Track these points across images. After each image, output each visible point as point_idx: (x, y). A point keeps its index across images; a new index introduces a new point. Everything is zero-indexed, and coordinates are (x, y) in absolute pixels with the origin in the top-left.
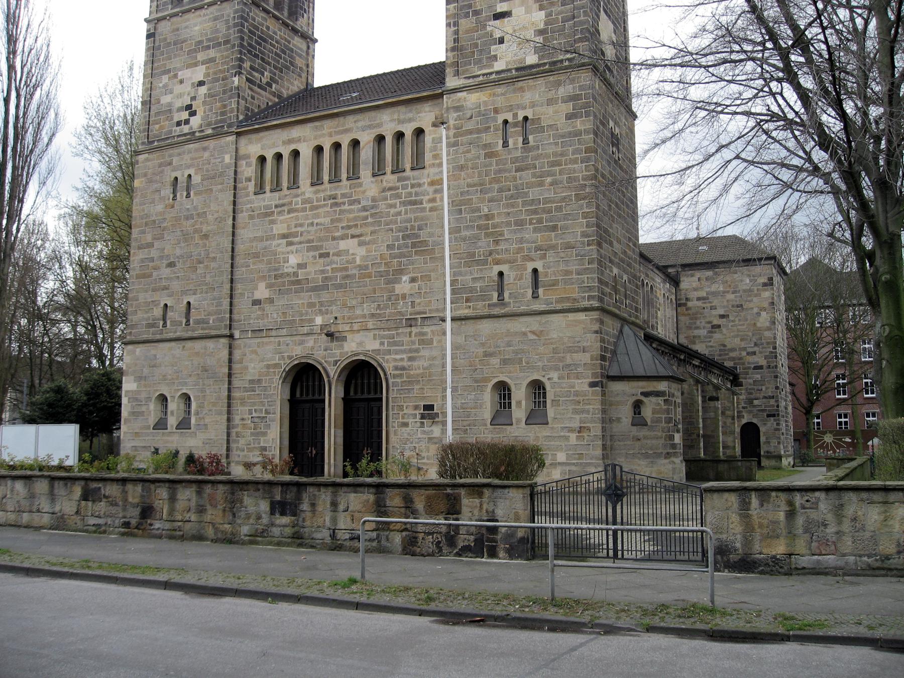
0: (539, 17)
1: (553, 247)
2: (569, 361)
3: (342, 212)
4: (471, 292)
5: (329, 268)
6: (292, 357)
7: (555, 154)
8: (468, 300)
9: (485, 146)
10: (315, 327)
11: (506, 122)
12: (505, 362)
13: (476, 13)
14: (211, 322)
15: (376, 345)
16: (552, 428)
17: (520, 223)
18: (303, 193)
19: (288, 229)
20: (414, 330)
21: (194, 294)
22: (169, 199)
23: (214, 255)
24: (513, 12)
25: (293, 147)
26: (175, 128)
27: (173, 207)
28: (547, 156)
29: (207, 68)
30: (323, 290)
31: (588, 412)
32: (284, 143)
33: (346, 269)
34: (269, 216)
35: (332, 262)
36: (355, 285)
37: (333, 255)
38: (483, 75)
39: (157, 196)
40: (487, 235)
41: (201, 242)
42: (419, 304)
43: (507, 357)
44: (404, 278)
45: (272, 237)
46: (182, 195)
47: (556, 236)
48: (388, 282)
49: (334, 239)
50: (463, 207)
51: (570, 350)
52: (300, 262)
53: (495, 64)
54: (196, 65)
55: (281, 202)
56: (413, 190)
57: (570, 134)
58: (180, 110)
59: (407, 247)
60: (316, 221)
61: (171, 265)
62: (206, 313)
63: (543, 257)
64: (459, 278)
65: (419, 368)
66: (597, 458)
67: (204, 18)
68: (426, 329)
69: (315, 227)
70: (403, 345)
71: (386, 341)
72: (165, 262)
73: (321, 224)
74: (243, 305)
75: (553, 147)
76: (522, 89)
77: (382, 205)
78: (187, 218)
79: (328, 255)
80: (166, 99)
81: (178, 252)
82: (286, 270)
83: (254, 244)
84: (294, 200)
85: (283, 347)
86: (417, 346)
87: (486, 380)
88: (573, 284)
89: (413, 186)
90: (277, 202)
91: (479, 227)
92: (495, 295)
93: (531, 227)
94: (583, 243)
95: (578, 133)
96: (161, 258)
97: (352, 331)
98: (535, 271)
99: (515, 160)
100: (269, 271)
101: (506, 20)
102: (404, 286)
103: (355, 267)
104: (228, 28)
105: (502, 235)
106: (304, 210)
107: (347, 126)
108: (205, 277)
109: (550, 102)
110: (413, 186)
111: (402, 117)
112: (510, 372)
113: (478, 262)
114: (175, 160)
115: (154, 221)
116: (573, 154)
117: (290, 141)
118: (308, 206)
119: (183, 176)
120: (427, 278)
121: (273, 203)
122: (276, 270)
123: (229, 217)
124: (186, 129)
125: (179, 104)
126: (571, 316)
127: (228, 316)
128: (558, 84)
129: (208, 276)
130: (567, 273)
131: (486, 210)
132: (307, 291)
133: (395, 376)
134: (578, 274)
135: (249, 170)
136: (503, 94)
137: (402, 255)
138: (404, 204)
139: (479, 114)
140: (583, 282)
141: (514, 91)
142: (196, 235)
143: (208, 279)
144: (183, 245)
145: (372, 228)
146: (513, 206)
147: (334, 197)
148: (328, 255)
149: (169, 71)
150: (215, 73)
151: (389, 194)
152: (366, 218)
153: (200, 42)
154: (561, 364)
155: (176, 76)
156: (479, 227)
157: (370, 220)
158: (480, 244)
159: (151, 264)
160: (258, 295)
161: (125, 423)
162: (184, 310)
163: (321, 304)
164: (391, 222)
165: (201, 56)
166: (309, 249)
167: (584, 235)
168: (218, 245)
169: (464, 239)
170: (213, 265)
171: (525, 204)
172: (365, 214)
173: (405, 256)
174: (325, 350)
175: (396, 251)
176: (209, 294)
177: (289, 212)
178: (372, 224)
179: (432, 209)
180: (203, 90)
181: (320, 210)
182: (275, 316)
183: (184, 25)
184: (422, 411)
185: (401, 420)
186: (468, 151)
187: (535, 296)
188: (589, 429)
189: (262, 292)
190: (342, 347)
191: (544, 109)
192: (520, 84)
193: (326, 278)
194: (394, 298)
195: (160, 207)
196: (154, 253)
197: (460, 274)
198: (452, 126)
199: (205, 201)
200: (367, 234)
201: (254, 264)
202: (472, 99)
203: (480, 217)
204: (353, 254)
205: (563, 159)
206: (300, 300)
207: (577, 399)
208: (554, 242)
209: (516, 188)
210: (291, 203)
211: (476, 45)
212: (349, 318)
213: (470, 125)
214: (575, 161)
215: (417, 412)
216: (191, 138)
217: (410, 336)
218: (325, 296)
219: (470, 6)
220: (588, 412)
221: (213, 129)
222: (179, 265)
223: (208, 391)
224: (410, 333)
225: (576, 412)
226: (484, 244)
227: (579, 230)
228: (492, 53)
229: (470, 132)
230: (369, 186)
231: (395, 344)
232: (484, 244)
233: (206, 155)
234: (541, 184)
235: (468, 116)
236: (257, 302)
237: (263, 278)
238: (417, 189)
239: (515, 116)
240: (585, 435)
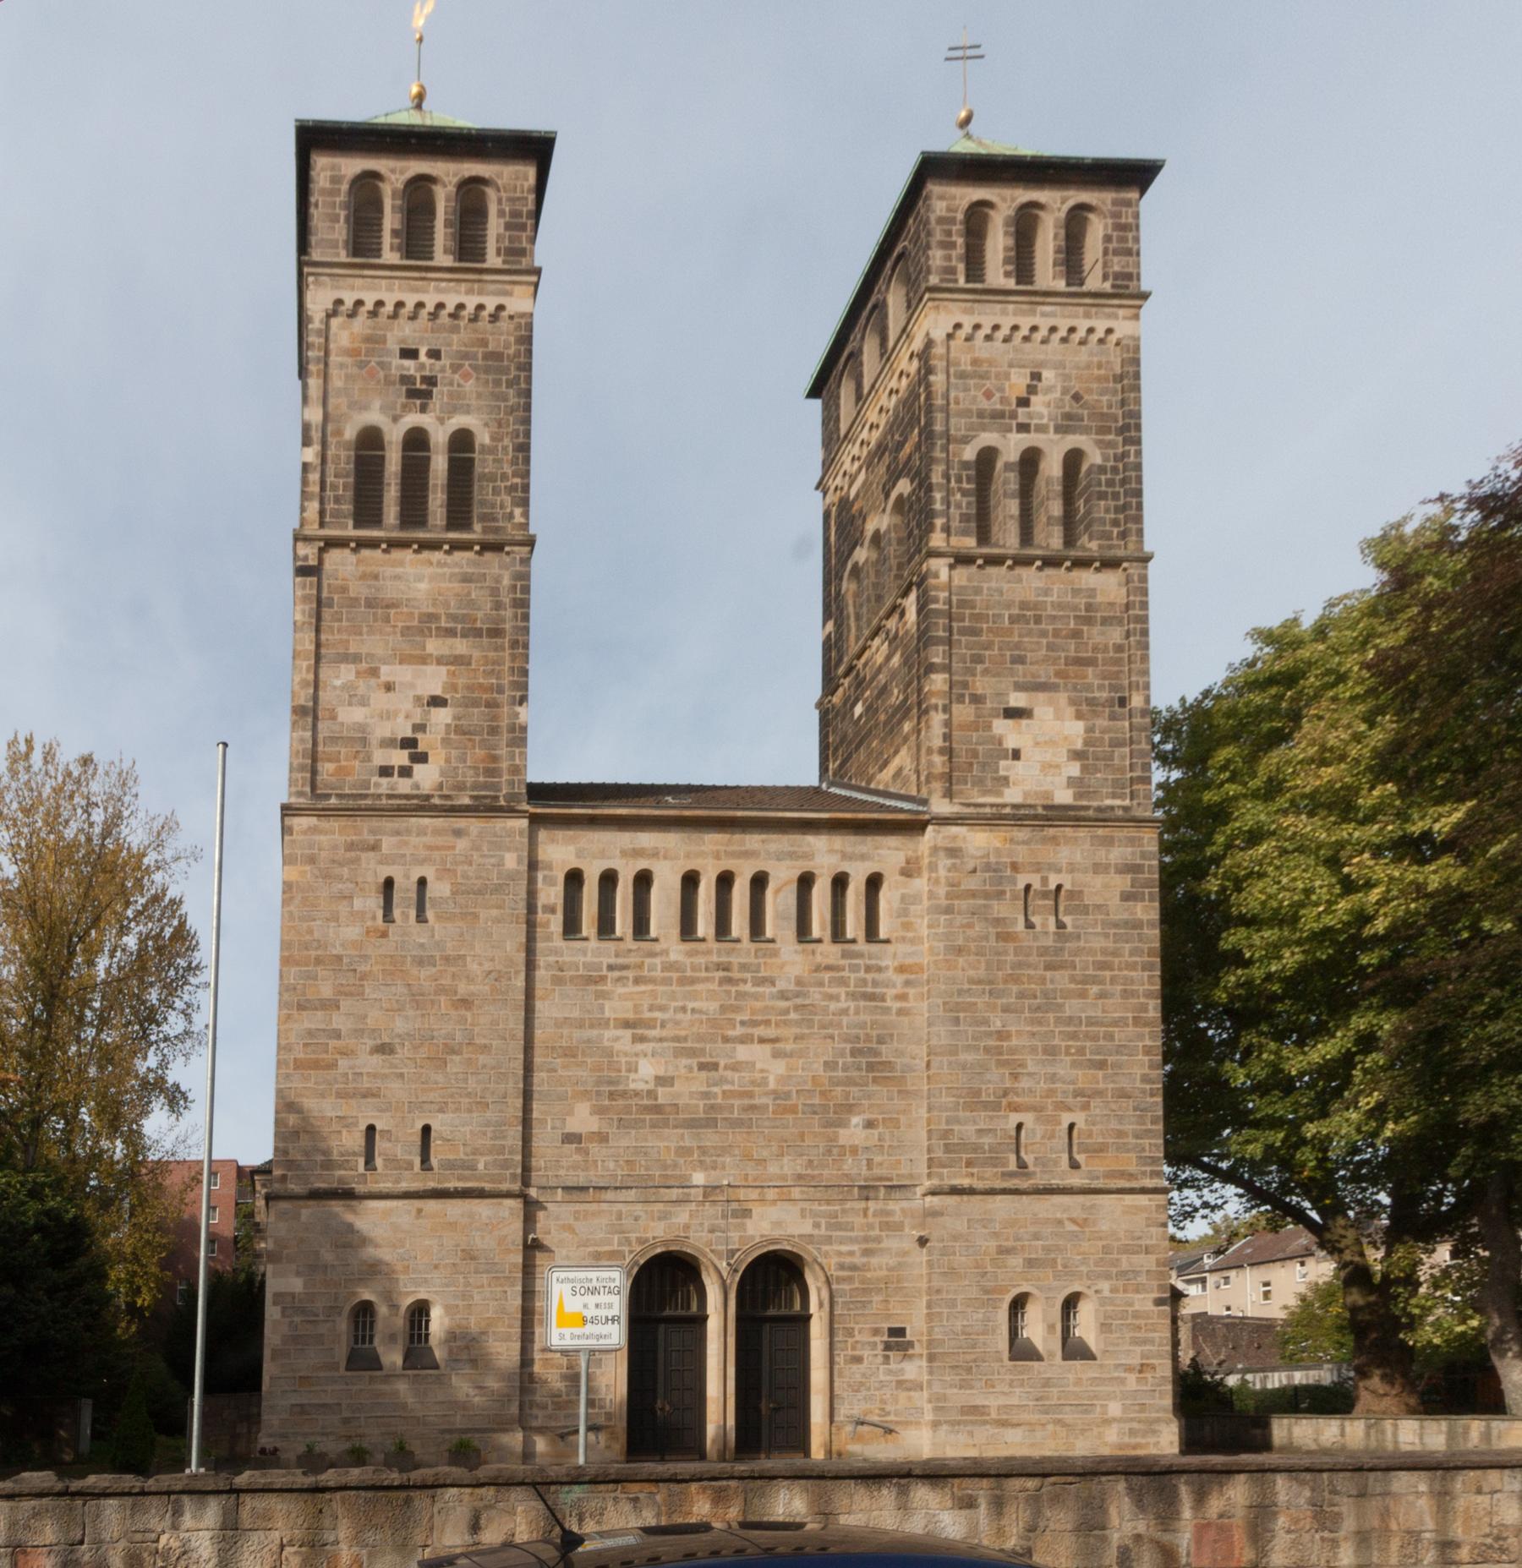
0: (1075, 730)
1: (1099, 1093)
2: (1125, 1266)
3: (741, 995)
4: (975, 1150)
5: (715, 1089)
6: (647, 1240)
7: (1104, 951)
8: (969, 1164)
9: (998, 921)
10: (693, 1191)
11: (1028, 888)
12: (1030, 1263)
13: (977, 699)
14: (481, 1166)
15: (806, 1228)
16: (1101, 1366)
17: (1051, 1051)
18: (666, 952)
19: (636, 1013)
20: (872, 1205)
21: (441, 1111)
22: (374, 918)
23: (484, 1041)
24: (1036, 712)
25: (642, 864)
26: (375, 779)
27: (384, 935)
28: (1091, 952)
29: (452, 674)
30: (706, 1126)
31: (1152, 1342)
32: (624, 853)
33: (750, 1095)
34: (596, 983)
35: (722, 1081)
36: (767, 1123)
37: (726, 1068)
38: (992, 805)
39: (343, 908)
40: (1001, 1064)
41: (453, 1012)
42: (881, 1164)
43: (1033, 1256)
44: (856, 1120)
45: (604, 1023)
46: (405, 916)
47: (1105, 1077)
48: (828, 1124)
49: (726, 1040)
50: (962, 1015)
51: (1127, 1250)
52: (661, 1073)
53: (1007, 791)
54: (423, 660)
55: (620, 961)
56: (869, 977)
57: (1126, 924)
58: (388, 743)
59: (859, 1069)
60: (690, 1005)
61: (384, 1049)
62: (468, 1150)
63: (1086, 1107)
64: (956, 1128)
65: (881, 1268)
66: (1165, 1410)
67: (440, 570)
68: (892, 1206)
69: (689, 1016)
70: (852, 1229)
71: (823, 1221)
72: (370, 1043)
73: (701, 1012)
74: (545, 1141)
75: (1102, 939)
76: (1054, 840)
77: (815, 996)
78: (420, 962)
79: (714, 1067)
80: (351, 715)
81: (400, 1026)
82: (632, 1086)
83: (565, 1032)
84: (648, 961)
85: (627, 1222)
86: (876, 1232)
87: (1003, 1290)
88: (1128, 1151)
89: (868, 969)
90: (612, 960)
91: (987, 1050)
92: (1013, 1158)
93: (1068, 1058)
94: (1143, 1091)
95: (1137, 925)
96: (359, 1033)
97: (762, 1200)
99: (1043, 952)
100: (599, 1082)
101: (1024, 722)
102: (854, 1132)
103: (766, 1094)
104: (498, 606)
105: (1023, 1065)
106: (666, 981)
107: (748, 846)
108: (466, 1080)
109: (1099, 868)
110: (868, 969)
111: (849, 849)
112: (1039, 1279)
113: (986, 1106)
114: (388, 844)
115: (339, 958)
116: (1131, 955)
117: (637, 853)
118: (675, 975)
119: (407, 877)
120: (893, 1123)
121: (606, 961)
122: (610, 1083)
123: (517, 972)
124: (404, 786)
125: (383, 730)
126: (1129, 1199)
127: (519, 1158)
128: (1108, 842)
129: (472, 1080)
130: (1121, 1134)
131: (999, 1024)
132: (675, 1127)
133: (840, 1280)
134: (1137, 1137)
135: (552, 894)
136: (1024, 843)
137: (850, 1082)
138: (853, 996)
139: (988, 867)
140: (1143, 1150)
141: (1045, 840)
142: (443, 998)
143: (472, 1084)
144: (411, 1013)
145: (796, 1030)
146: (1040, 1023)
147: (726, 968)
148: (714, 1067)
149: (356, 658)
150: (470, 688)
151: (827, 976)
152: (787, 1011)
153: (432, 617)
154: (1114, 1270)
155: (374, 672)
156: (987, 1050)
157: (793, 1016)
158: (988, 1077)
159: (333, 1043)
160: (574, 1125)
161: (273, 1359)
162: (417, 1139)
163: (703, 1150)
164: (831, 1024)
165: (433, 646)
166: (679, 1053)
167: (1145, 1079)
168: (494, 1023)
169: (964, 1067)
170: (482, 1059)
171: (1058, 1021)
172: (783, 1004)
173: (856, 1084)
174: (712, 1231)
175: (840, 1074)
176: (475, 1115)
177: (637, 981)
178: (798, 1023)
179: (901, 1012)
180: (442, 717)
181: (699, 987)
182: (612, 1165)
183: (389, 571)
184: (885, 1338)
185: (850, 1352)
186: (970, 926)
188: (1154, 1368)
189: (583, 1119)
190: (743, 1227)
191: (1089, 878)
192: (1051, 831)
193: (712, 1107)
194: (835, 1151)
195: (352, 932)
196: (339, 1021)
197: (958, 1121)
198: (943, 881)
199: (462, 935)
200: (786, 1040)
201: (564, 1067)
202: (977, 841)
203: (989, 1034)
204: (762, 1071)
205: (1117, 960)
206: (665, 1143)
207: (1137, 1322)
208: (1101, 1086)
209: (1045, 995)
210: (640, 966)
211: (975, 754)
212: (755, 1180)
213: (972, 883)
214: (1132, 966)
215: (877, 1339)
216: (422, 806)
217: (865, 1215)
218: (710, 1138)
220: (1152, 1342)
221: (472, 797)
222: (403, 1052)
223: (477, 1298)
224: (866, 1210)
225: (1135, 1342)
226: (996, 1078)
227: (1138, 1072)
228: (1002, 773)
229: (973, 894)
230: (791, 959)
231: (839, 1227)
232: (996, 1078)
233: (462, 844)
234: (1083, 995)
235: (970, 866)
236: (571, 1138)
237: (585, 1095)
238: (876, 976)
239: (1045, 881)
240: (1149, 1375)
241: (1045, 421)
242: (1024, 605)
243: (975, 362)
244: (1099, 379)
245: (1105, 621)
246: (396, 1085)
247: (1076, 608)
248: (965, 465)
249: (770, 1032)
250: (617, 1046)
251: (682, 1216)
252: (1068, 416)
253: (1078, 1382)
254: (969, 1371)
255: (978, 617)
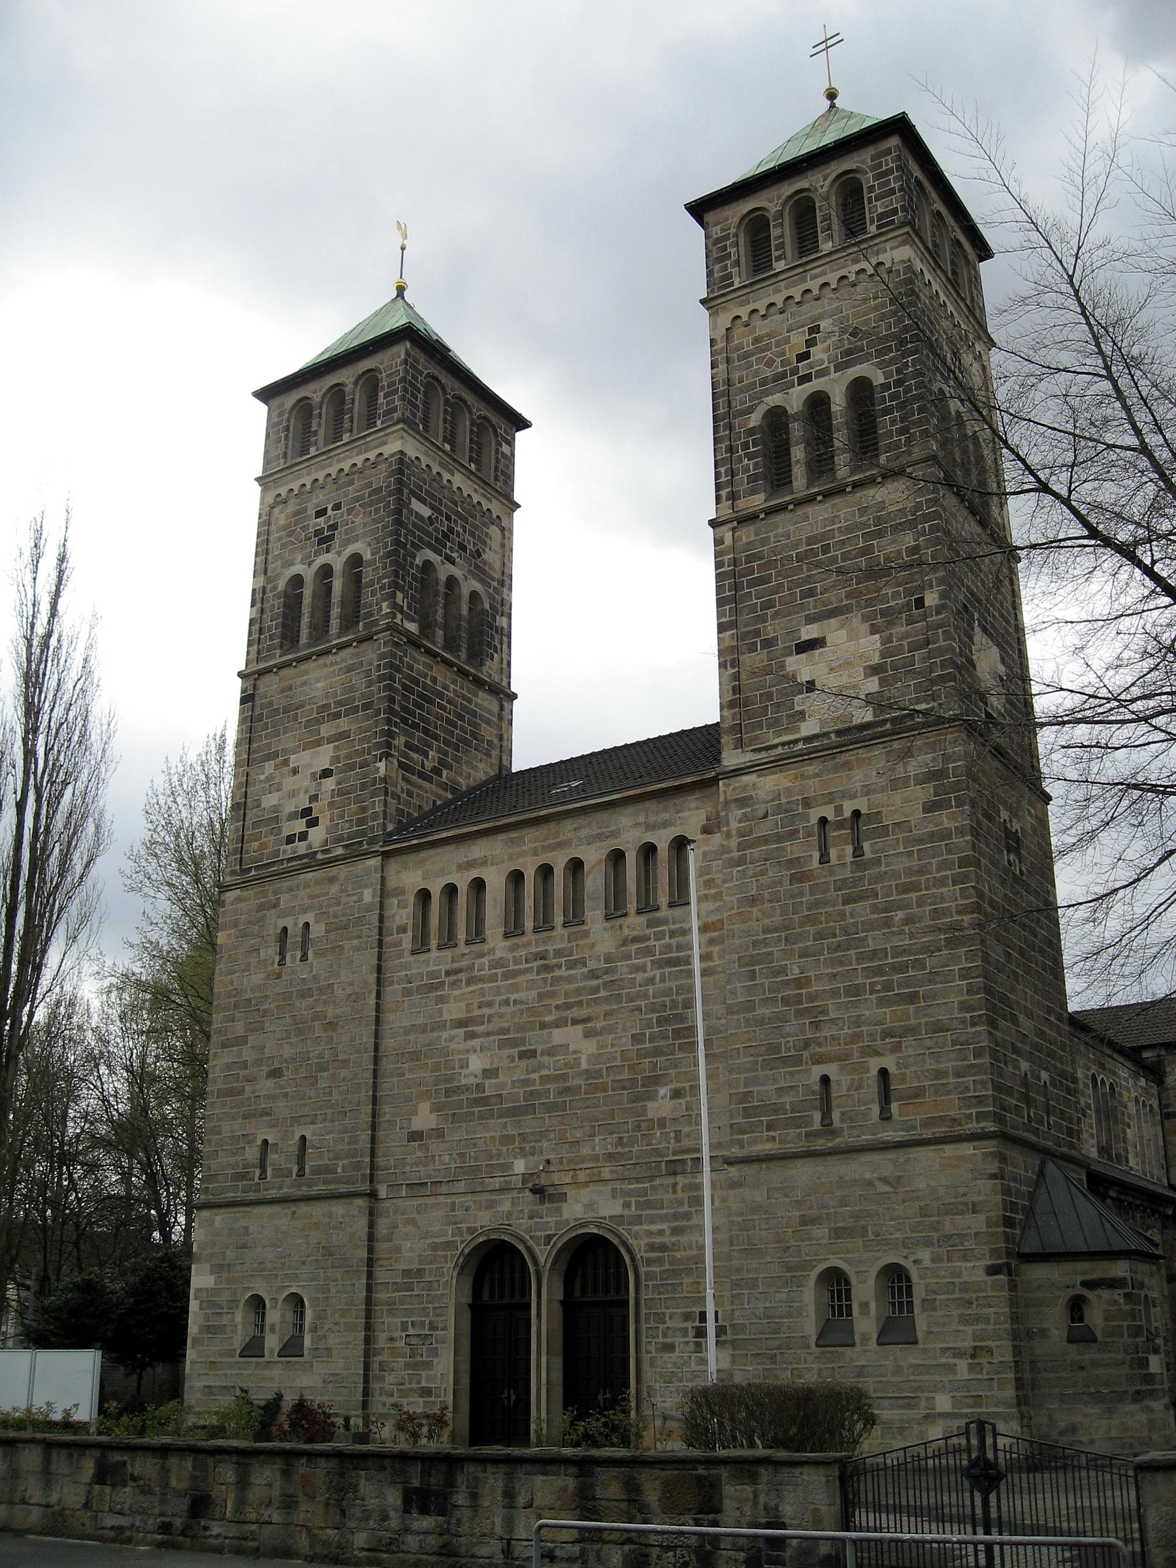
0: (870, 645)
1: (912, 1031)
2: (948, 1229)
3: (556, 980)
4: (775, 1112)
5: (535, 1076)
6: (476, 1230)
7: (909, 872)
8: (770, 1127)
10: (513, 1178)
11: (823, 821)
12: (837, 1233)
13: (768, 643)
14: (339, 1170)
16: (925, 1350)
17: (854, 991)
18: (492, 951)
19: (467, 1012)
20: (681, 1180)
21: (313, 1123)
22: (273, 963)
23: (345, 1057)
24: (828, 639)
25: (475, 873)
26: (285, 847)
27: (279, 976)
28: (895, 875)
29: (337, 748)
30: (526, 1114)
31: (987, 1320)
33: (564, 1077)
34: (437, 989)
35: (540, 1067)
36: (579, 1104)
37: (542, 1054)
38: (783, 744)
39: (253, 960)
40: (799, 1014)
41: (323, 1035)
42: (688, 1135)
43: (841, 1225)
44: (663, 1091)
45: (442, 1026)
46: (293, 957)
47: (917, 1011)
48: (637, 1098)
49: (543, 1026)
50: (757, 967)
51: (951, 1210)
52: (488, 1066)
53: (803, 725)
54: (318, 743)
55: (456, 965)
56: (673, 941)
57: (932, 836)
58: (293, 816)
59: (666, 1038)
60: (513, 997)
61: (275, 1073)
62: (331, 1155)
63: (897, 1048)
64: (755, 1089)
65: (691, 1247)
66: (1006, 1404)
67: (331, 669)
69: (512, 1008)
70: (662, 1208)
71: (633, 1200)
72: (266, 1069)
73: (521, 1002)
74: (393, 1142)
75: (905, 859)
76: (848, 766)
78: (303, 995)
79: (532, 1054)
80: (270, 800)
81: (287, 1052)
82: (464, 1082)
83: (411, 1038)
84: (477, 962)
85: (459, 1213)
86: (686, 1208)
87: (808, 1265)
88: (948, 1093)
89: (672, 934)
90: (448, 967)
91: (786, 1001)
92: (817, 1116)
93: (873, 997)
94: (963, 1021)
95: (946, 835)
96: (259, 1062)
97: (575, 1184)
98: (883, 1072)
99: (841, 885)
100: (437, 1082)
103: (579, 1074)
104: (370, 684)
105: (824, 1012)
106: (493, 978)
107: (562, 838)
108: (330, 1094)
109: (894, 785)
110: (672, 934)
111: (652, 819)
112: (848, 1252)
113: (787, 1061)
114: (284, 900)
115: (249, 1001)
116: (939, 870)
117: (470, 865)
118: (499, 971)
119: (296, 924)
121: (443, 968)
122: (447, 1081)
123: (370, 992)
124: (301, 847)
125: (290, 807)
126: (949, 1150)
127: (368, 1159)
128: (908, 753)
129: (335, 1093)
130: (939, 1074)
131: (796, 971)
132: (500, 1117)
133: (649, 1262)
134: (958, 1075)
135: (402, 914)
136: (816, 775)
137: (657, 1052)
138: (659, 964)
139: (779, 809)
140: (967, 1089)
141: (836, 769)
142: (316, 1023)
143: (336, 1097)
144: (294, 1040)
145: (606, 1007)
146: (841, 963)
147: (542, 956)
148: (532, 1054)
149: (276, 755)
150: (349, 756)
151: (633, 948)
152: (596, 990)
153: (325, 707)
154: (935, 1235)
155: (286, 762)
156: (786, 1001)
157: (603, 993)
158: (788, 1029)
159: (243, 1073)
160: (418, 1124)
161: (193, 1346)
162: (295, 1150)
163: (523, 1137)
164: (638, 996)
165: (326, 730)
166: (503, 1045)
167: (965, 1007)
168: (352, 1040)
169: (760, 1022)
170: (344, 1073)
171: (861, 957)
172: (595, 982)
173: (663, 1054)
174: (531, 1217)
175: (648, 1045)
176: (336, 1123)
177: (469, 982)
178: (607, 1000)
180: (330, 784)
181: (521, 979)
182: (447, 1159)
183: (299, 680)
185: (661, 1340)
186: (763, 873)
187: (886, 1116)
188: (990, 1351)
189: (424, 1118)
190: (558, 1211)
192: (844, 758)
193: (531, 1093)
195: (258, 978)
196: (247, 1054)
197: (756, 1081)
198: (734, 832)
199: (331, 967)
200: (597, 1018)
201: (411, 1070)
202: (766, 785)
203: (786, 983)
204: (575, 1052)
205: (923, 878)
206: (489, 1132)
207: (966, 1296)
208: (913, 1021)
209: (846, 931)
210: (471, 968)
211: (769, 696)
212: (570, 1162)
213: (764, 830)
214: (942, 882)
215: (689, 1325)
216: (310, 861)
217: (674, 1192)
218: (530, 1124)
219: (757, 633)
220: (987, 1320)
221: (344, 846)
222: (288, 1075)
223: (333, 1290)
224: (674, 1186)
225: (964, 1320)
226: (795, 1030)
227: (956, 999)
228: (797, 708)
229: (765, 840)
231: (649, 1205)
232: (795, 1030)
233: (334, 889)
234: (888, 923)
235: (761, 813)
236: (415, 1136)
238: (679, 939)
239: (839, 810)
240: (983, 1361)
241: (826, 364)
242: (811, 540)
243: (756, 340)
244: (876, 308)
245: (896, 529)
246: (281, 1103)
247: (865, 525)
248: (751, 431)
249: (583, 1013)
250: (453, 1046)
251: (505, 1204)
252: (848, 352)
253: (898, 1370)
254: (773, 1358)
255: (770, 564)
